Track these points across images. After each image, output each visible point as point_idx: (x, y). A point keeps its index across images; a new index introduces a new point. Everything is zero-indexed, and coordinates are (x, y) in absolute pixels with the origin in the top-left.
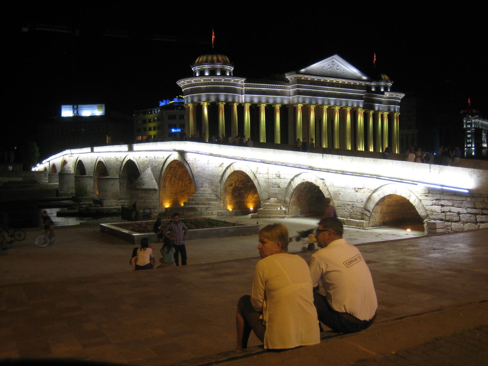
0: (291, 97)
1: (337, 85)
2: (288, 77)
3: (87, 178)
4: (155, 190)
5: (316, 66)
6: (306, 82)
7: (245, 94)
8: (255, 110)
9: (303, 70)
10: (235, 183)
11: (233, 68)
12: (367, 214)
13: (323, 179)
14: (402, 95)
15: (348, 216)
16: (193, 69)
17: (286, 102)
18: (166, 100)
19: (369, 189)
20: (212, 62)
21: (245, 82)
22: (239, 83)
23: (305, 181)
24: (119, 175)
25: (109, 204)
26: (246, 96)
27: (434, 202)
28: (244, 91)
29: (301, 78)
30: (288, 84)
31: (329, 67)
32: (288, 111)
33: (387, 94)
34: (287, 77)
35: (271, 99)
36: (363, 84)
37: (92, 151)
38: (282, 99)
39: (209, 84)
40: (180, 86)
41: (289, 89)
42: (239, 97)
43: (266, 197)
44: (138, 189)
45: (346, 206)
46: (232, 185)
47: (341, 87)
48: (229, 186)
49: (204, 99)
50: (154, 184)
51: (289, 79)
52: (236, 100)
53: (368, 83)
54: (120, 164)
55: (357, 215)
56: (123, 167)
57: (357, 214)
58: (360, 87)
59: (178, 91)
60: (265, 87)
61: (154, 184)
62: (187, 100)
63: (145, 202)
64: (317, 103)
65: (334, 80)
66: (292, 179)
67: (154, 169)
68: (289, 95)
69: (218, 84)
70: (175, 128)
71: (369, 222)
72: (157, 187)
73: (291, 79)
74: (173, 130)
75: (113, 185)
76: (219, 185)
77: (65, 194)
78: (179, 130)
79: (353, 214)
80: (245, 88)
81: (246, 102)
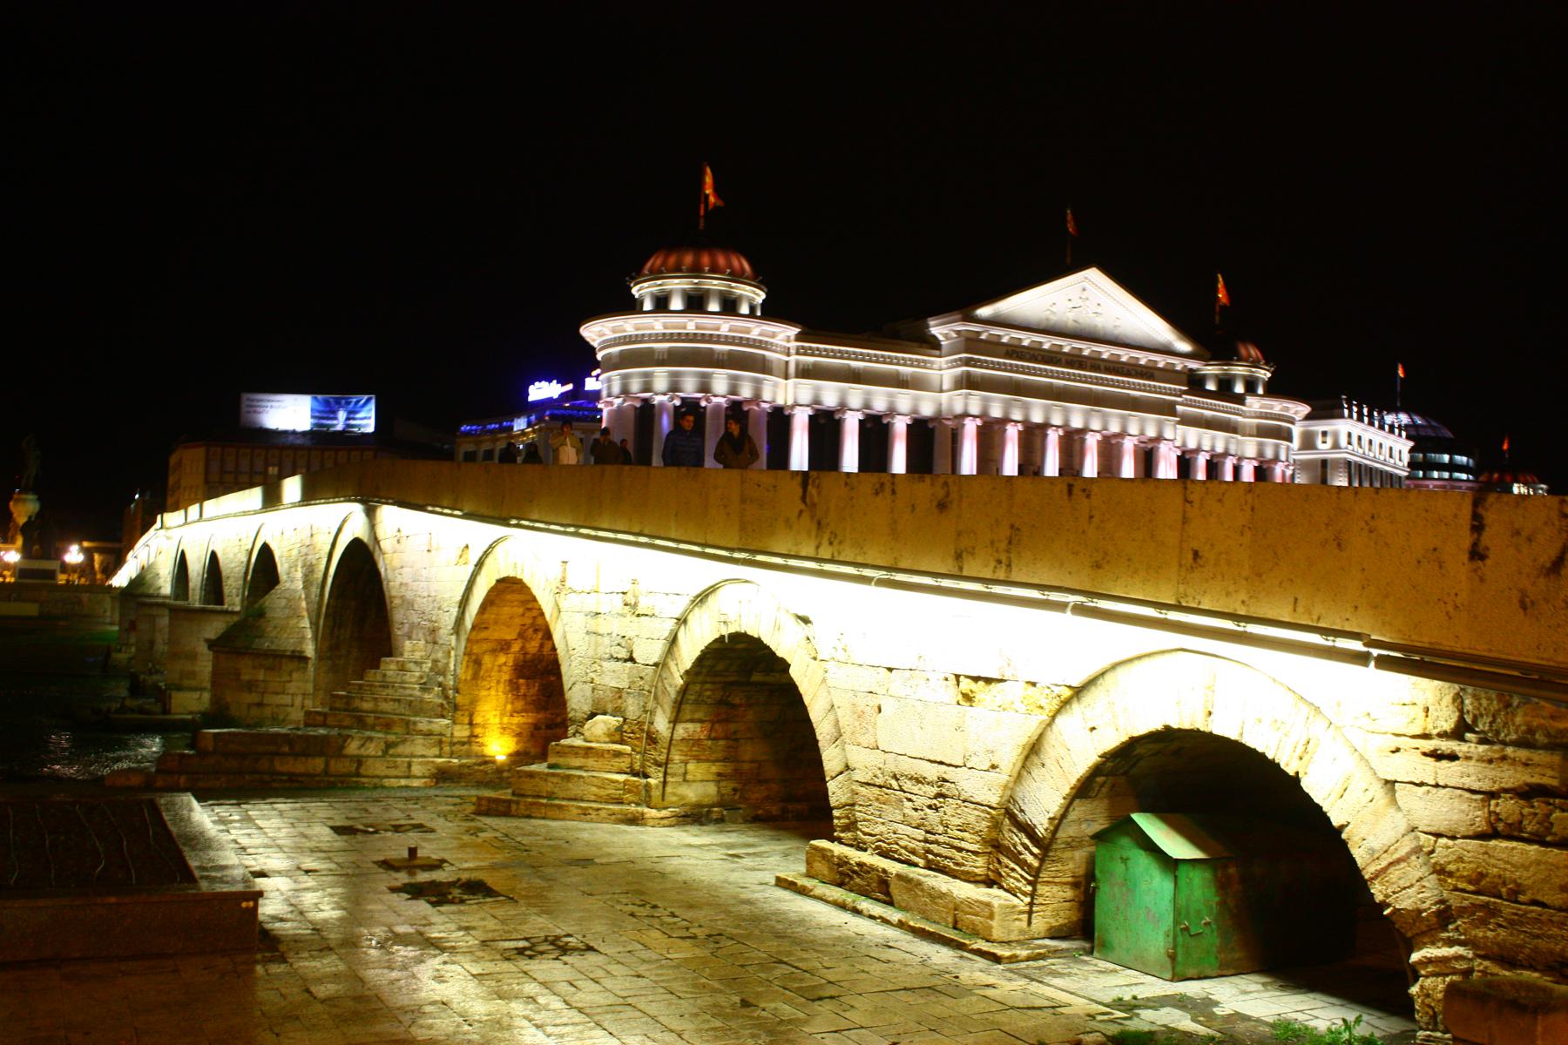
0: (944, 395)
1: (1094, 364)
2: (939, 329)
6: (993, 347)
7: (797, 376)
8: (825, 427)
9: (984, 312)
10: (521, 635)
11: (763, 296)
12: (1020, 848)
13: (806, 621)
15: (913, 852)
16: (635, 291)
17: (927, 410)
19: (1034, 684)
20: (696, 271)
22: (779, 340)
23: (732, 630)
27: (1507, 807)
29: (979, 333)
31: (1071, 305)
32: (930, 439)
33: (1254, 404)
35: (880, 399)
36: (1179, 364)
42: (775, 385)
43: (587, 708)
45: (908, 785)
46: (504, 646)
47: (1109, 371)
48: (493, 651)
51: (941, 338)
53: (1193, 365)
55: (960, 850)
57: (963, 845)
63: (260, 705)
65: (1087, 349)
66: (682, 621)
71: (1031, 904)
72: (310, 650)
73: (946, 336)
76: (453, 643)
79: (941, 839)
81: (796, 404)
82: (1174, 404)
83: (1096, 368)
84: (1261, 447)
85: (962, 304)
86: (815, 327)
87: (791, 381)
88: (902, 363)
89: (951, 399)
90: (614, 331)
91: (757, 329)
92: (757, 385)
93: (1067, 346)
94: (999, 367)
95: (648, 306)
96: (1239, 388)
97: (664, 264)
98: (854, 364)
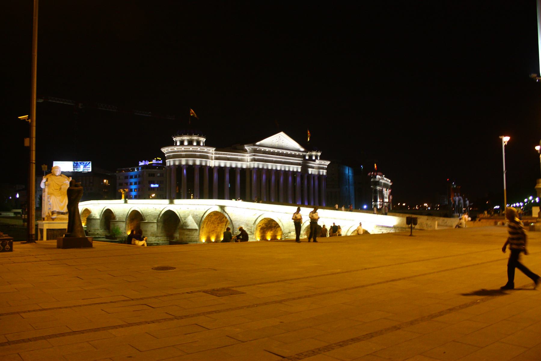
1: (282, 154)
2: (247, 148)
4: (196, 230)
5: (268, 141)
9: (258, 143)
14: (328, 163)
18: (145, 161)
24: (158, 220)
25: (150, 240)
28: (213, 158)
33: (318, 162)
37: (126, 202)
38: (242, 164)
39: (188, 151)
44: (184, 229)
50: (195, 226)
53: (304, 154)
54: (159, 213)
56: (161, 215)
58: (299, 156)
59: (162, 155)
60: (229, 155)
61: (195, 226)
62: (170, 163)
65: (281, 151)
67: (194, 217)
69: (195, 151)
70: (154, 184)
72: (197, 228)
74: (152, 186)
75: (152, 226)
77: (93, 234)
78: (157, 186)
85: (252, 142)
87: (213, 161)
88: (238, 156)
89: (250, 164)
91: (206, 149)
92: (206, 161)
93: (276, 150)
94: (261, 156)
95: (178, 144)
96: (314, 158)
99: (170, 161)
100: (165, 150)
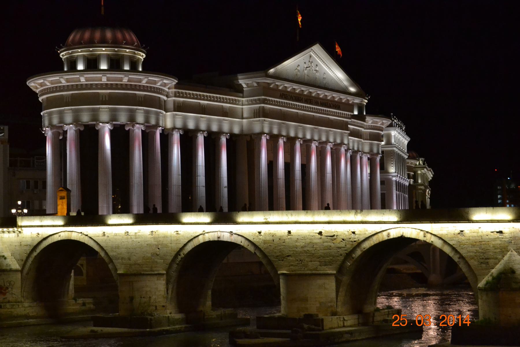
0: (244, 120)
2: (243, 81)
3: (149, 277)
5: (290, 65)
7: (175, 111)
9: (272, 71)
20: (115, 43)
21: (175, 88)
24: (340, 270)
26: (176, 115)
28: (171, 105)
29: (269, 84)
30: (241, 95)
32: (242, 146)
34: (241, 82)
35: (215, 123)
40: (34, 90)
41: (243, 105)
49: (104, 116)
51: (244, 86)
52: (161, 123)
56: (358, 252)
64: (288, 133)
65: (314, 92)
68: (241, 117)
80: (174, 98)
81: (174, 128)
82: (347, 123)
83: (317, 104)
84: (371, 145)
86: (186, 81)
89: (251, 123)
90: (67, 81)
96: (356, 113)
97: (82, 38)
98: (202, 102)
99: (61, 113)
100: (35, 84)
